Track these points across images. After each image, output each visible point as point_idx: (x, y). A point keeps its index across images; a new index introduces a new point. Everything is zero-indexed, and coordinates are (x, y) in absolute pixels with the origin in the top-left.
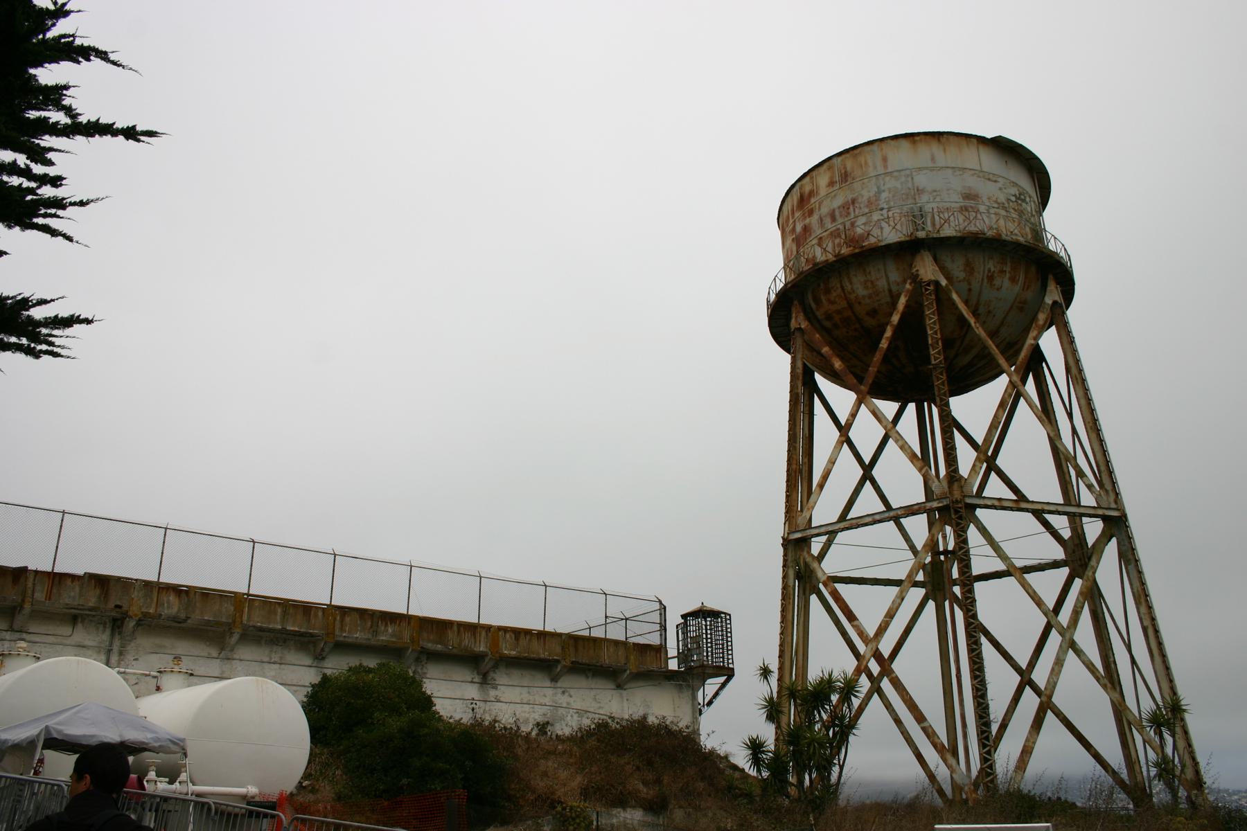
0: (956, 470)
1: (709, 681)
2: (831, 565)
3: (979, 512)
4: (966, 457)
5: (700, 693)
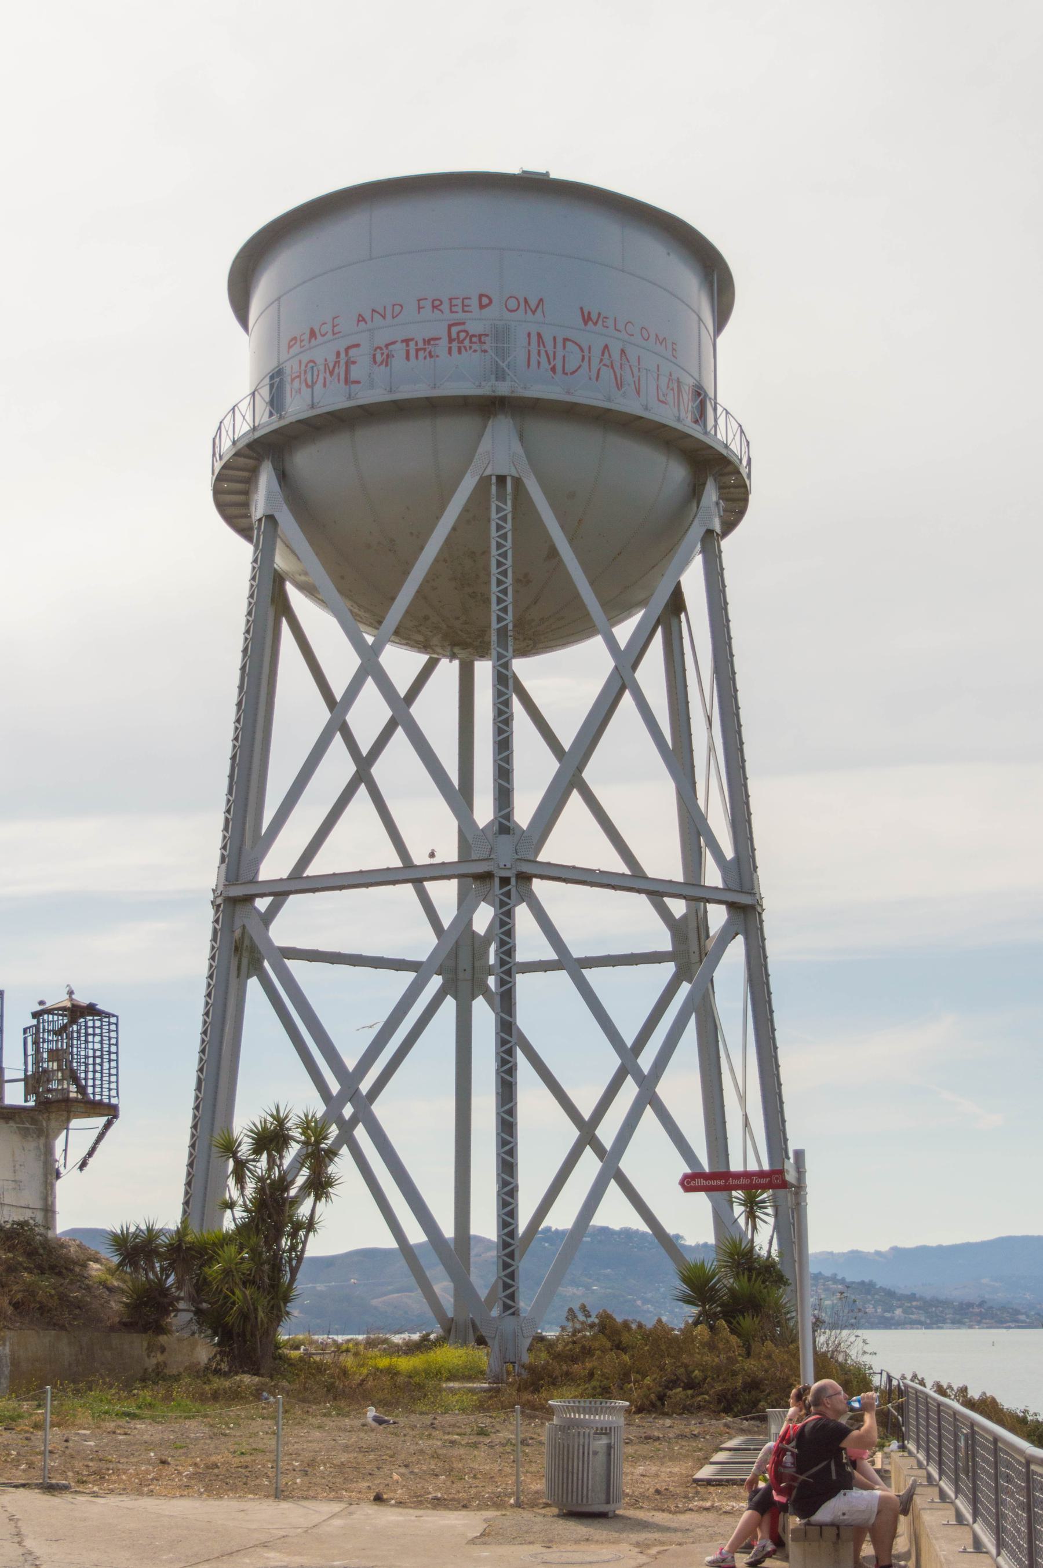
0: (508, 817)
1: (75, 1123)
2: (283, 932)
3: (538, 886)
4: (534, 769)
5: (59, 1143)
